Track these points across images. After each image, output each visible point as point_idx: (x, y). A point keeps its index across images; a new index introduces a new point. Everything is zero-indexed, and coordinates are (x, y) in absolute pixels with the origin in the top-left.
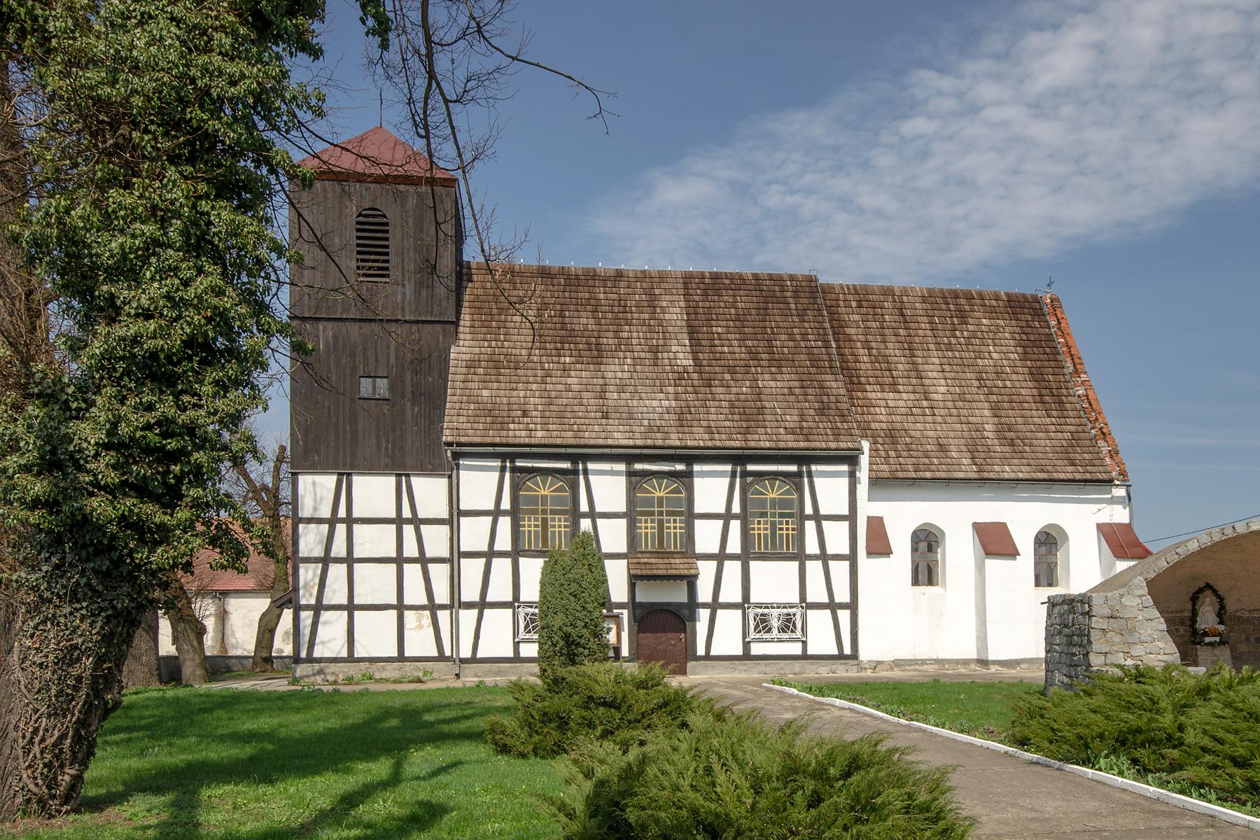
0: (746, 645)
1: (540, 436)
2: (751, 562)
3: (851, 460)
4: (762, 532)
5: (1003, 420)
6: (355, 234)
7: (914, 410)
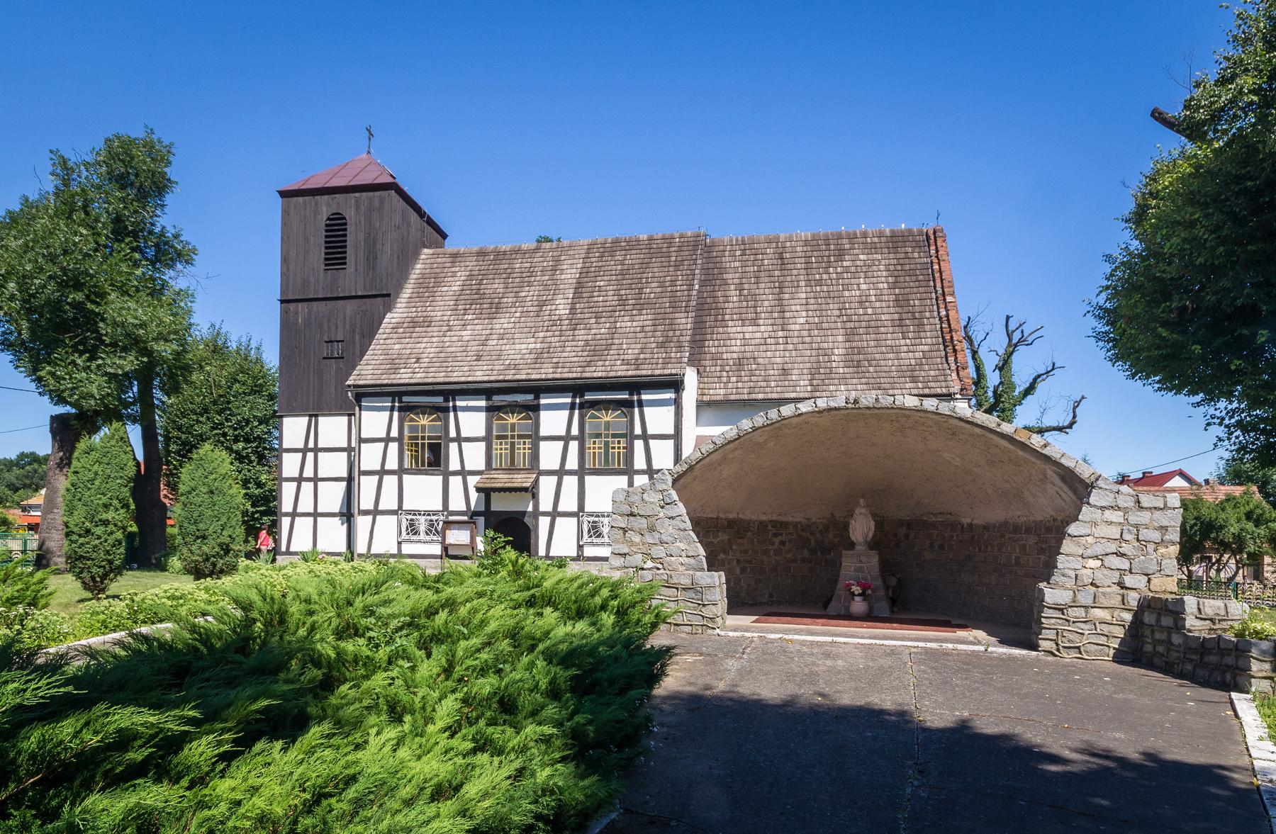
0: (580, 547)
1: (419, 377)
2: (586, 477)
3: (675, 385)
4: (597, 451)
5: (854, 344)
6: (324, 233)
7: (769, 341)
